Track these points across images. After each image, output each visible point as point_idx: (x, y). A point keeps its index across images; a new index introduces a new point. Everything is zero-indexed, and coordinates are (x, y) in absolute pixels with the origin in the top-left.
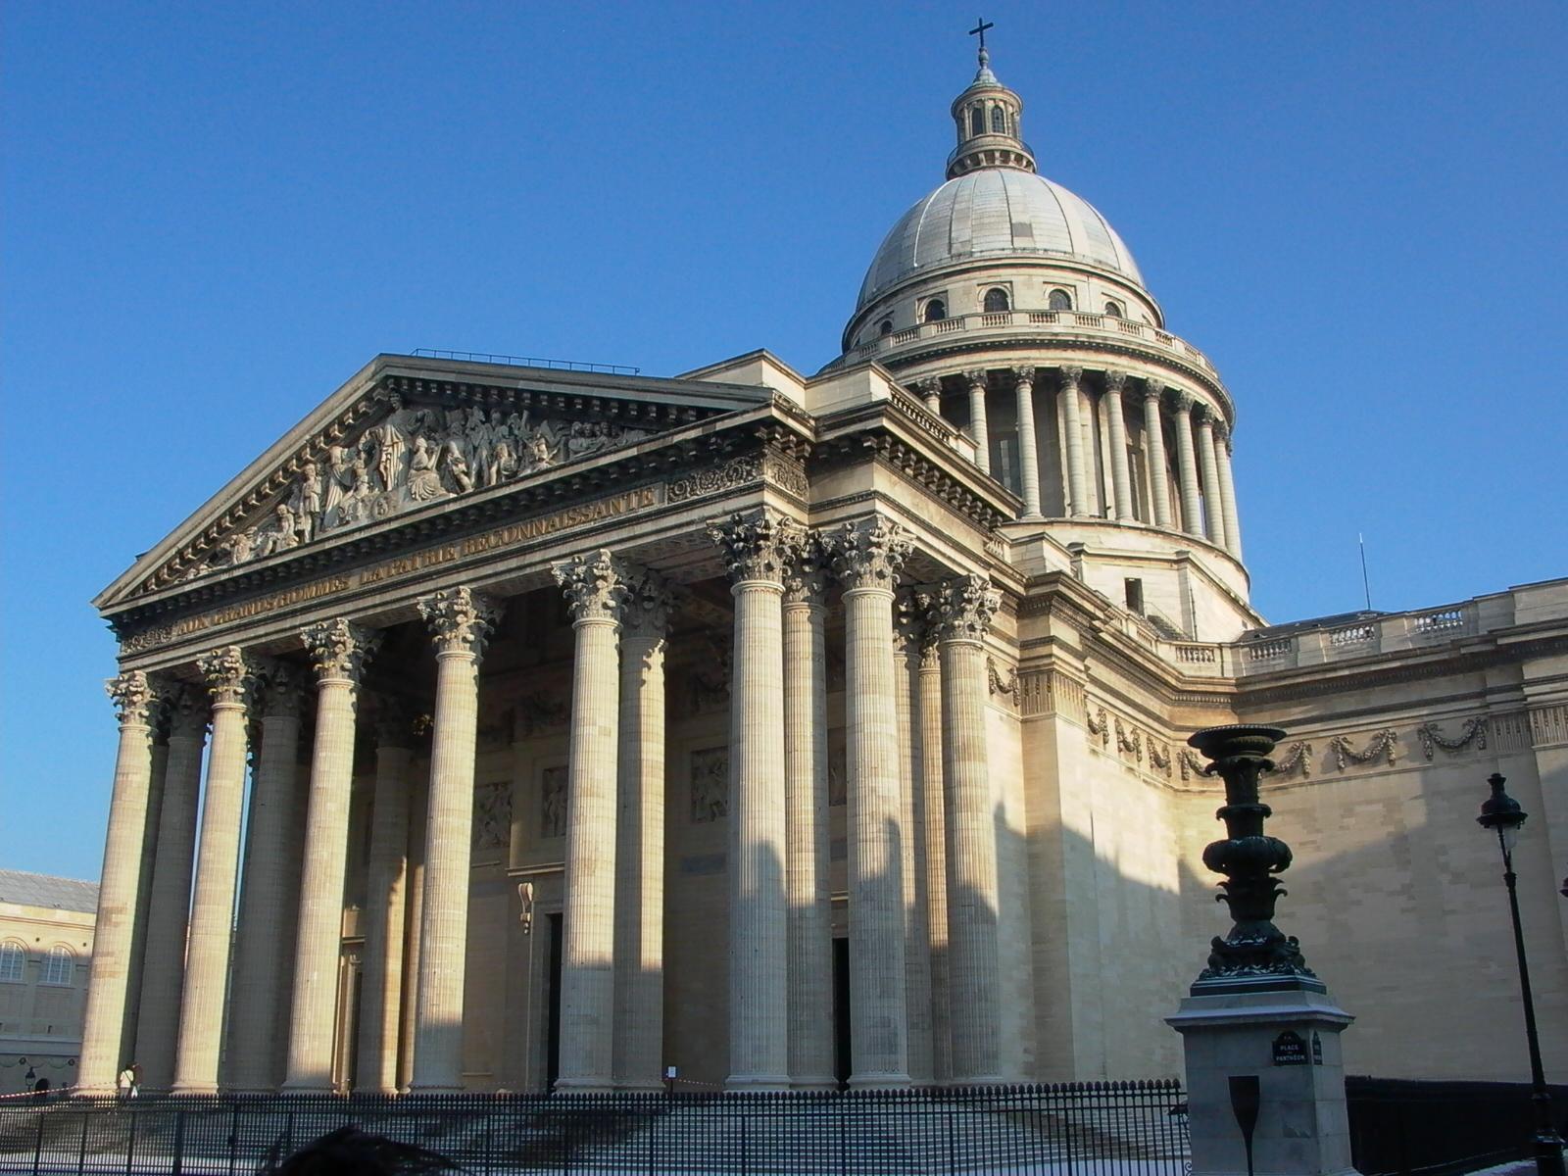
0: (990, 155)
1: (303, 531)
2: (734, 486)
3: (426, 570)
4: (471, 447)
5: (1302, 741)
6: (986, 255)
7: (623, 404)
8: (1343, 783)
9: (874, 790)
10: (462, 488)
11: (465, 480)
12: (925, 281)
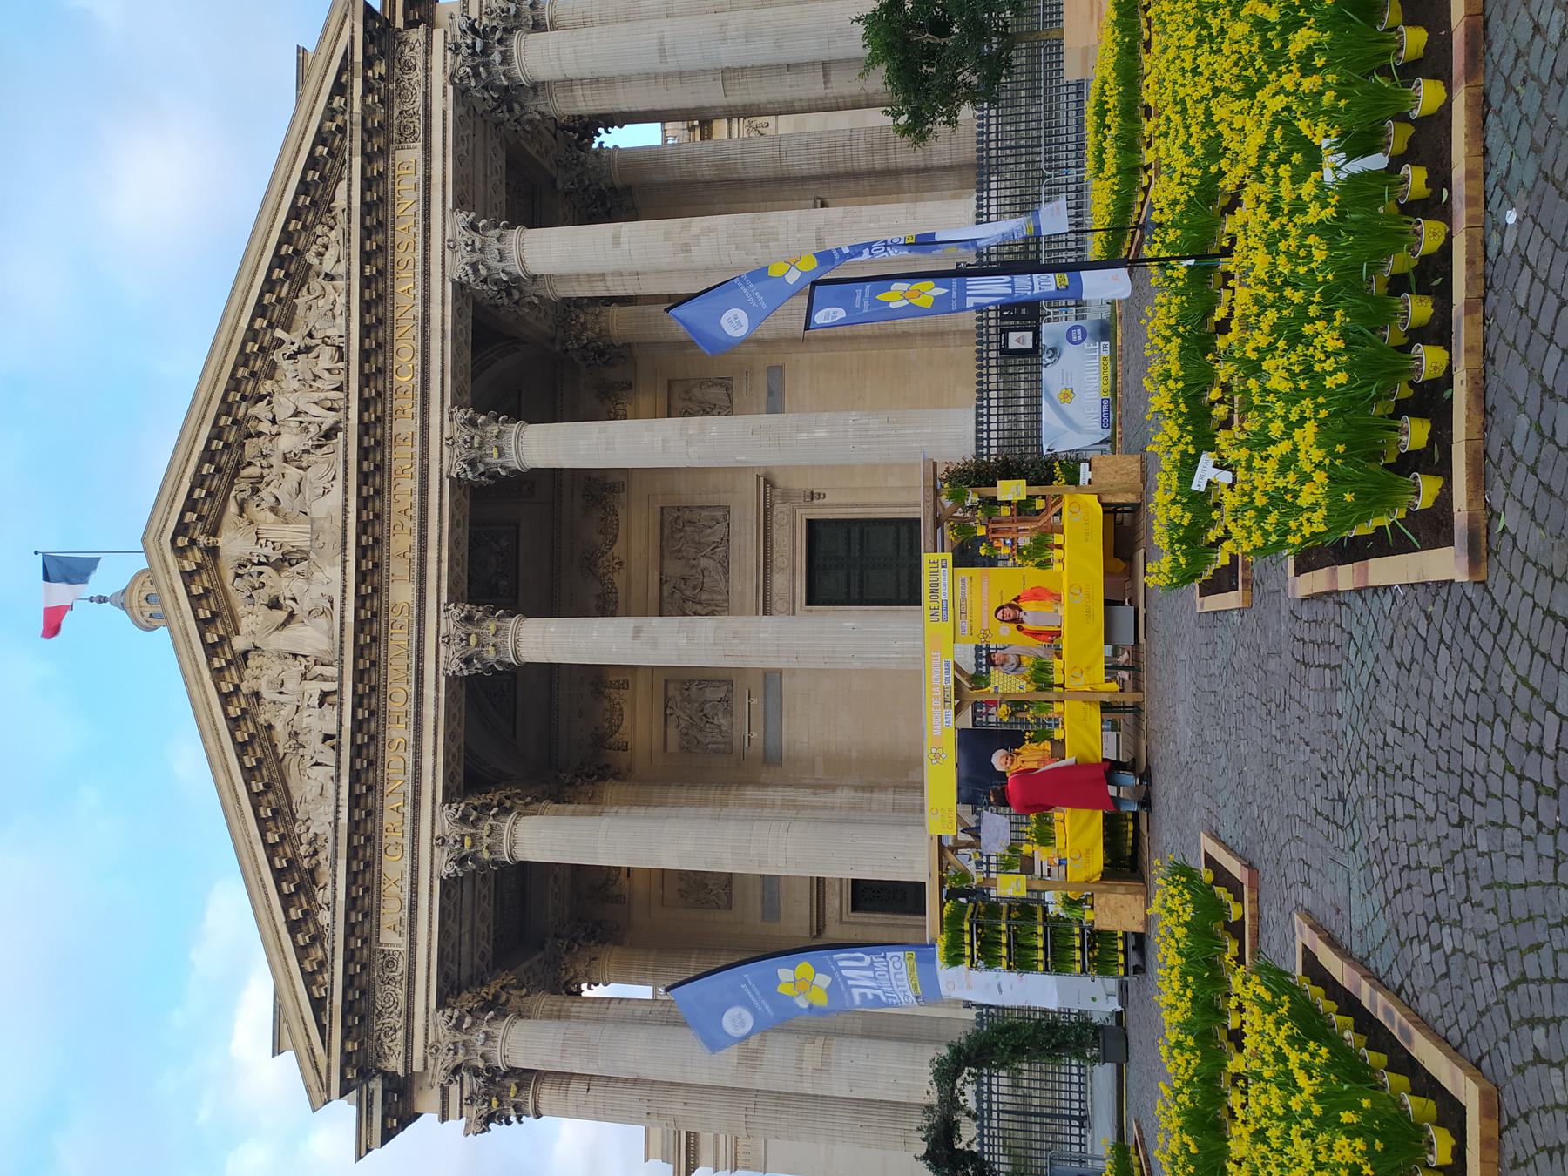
1: (324, 695)
2: (420, 64)
3: (417, 476)
4: (293, 423)
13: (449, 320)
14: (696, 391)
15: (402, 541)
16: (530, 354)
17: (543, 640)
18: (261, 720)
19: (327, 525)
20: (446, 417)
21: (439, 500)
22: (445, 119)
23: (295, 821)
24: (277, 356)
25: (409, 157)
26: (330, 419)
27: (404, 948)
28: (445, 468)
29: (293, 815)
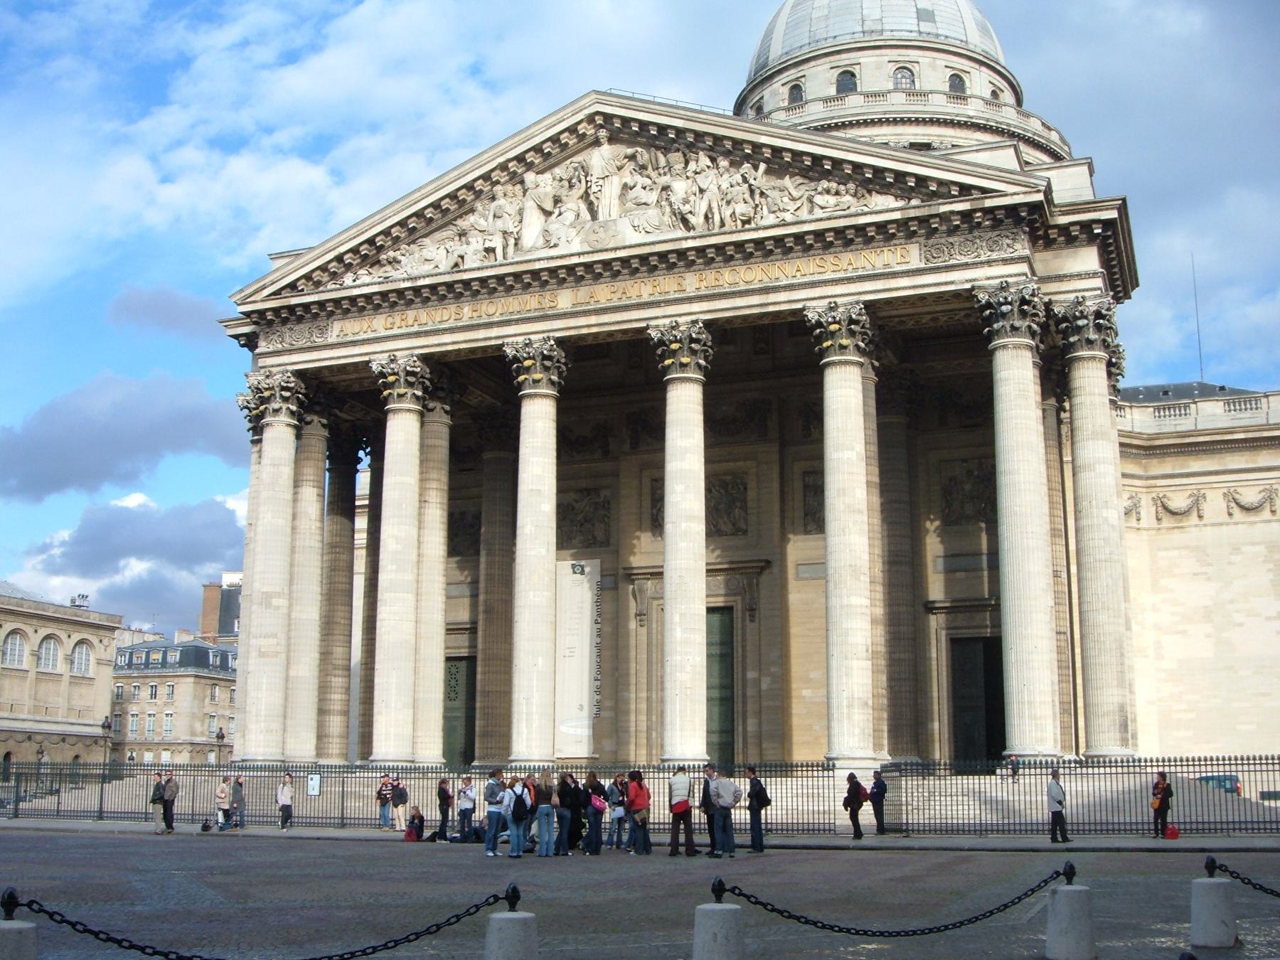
2: (994, 256)
3: (652, 299)
4: (695, 189)
5: (1199, 490)
6: (897, 35)
8: (1232, 527)
9: (1106, 519)
11: (692, 220)
12: (839, 52)
13: (777, 308)
15: (604, 293)
16: (765, 376)
18: (478, 205)
19: (611, 233)
20: (694, 317)
21: (631, 319)
22: (946, 283)
25: (913, 255)
28: (653, 323)
29: (414, 242)
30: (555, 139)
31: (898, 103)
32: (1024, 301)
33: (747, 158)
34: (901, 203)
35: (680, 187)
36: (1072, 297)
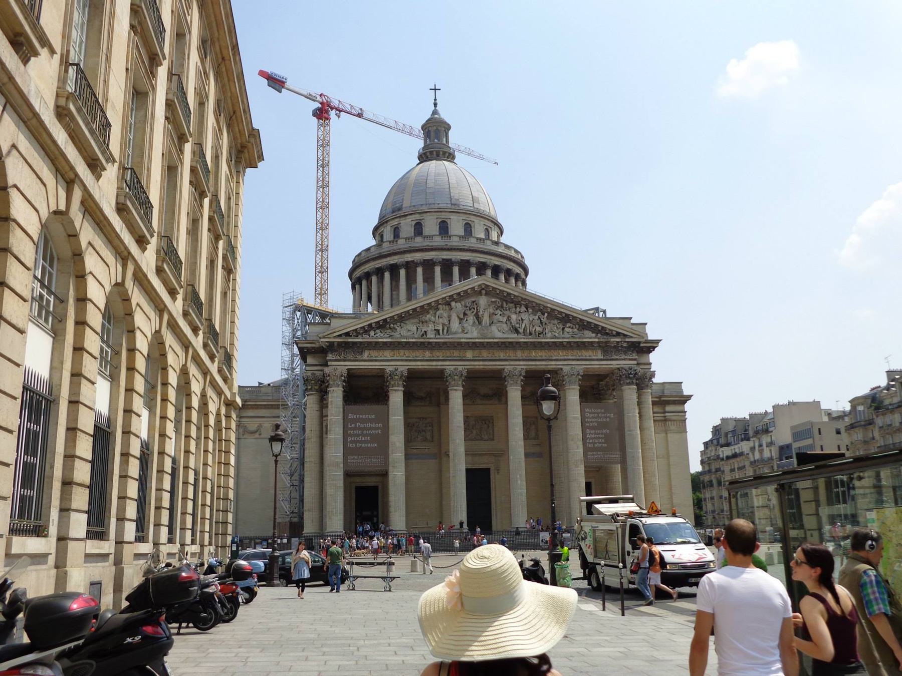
0: (444, 153)
1: (438, 331)
7: (588, 322)
10: (517, 332)
14: (533, 427)
15: (485, 354)
17: (456, 397)
21: (497, 365)
23: (401, 322)
24: (539, 314)
26: (521, 330)
27: (365, 357)
30: (466, 291)
31: (472, 243)
32: (636, 374)
33: (540, 310)
34: (594, 335)
35: (514, 317)
36: (642, 371)
